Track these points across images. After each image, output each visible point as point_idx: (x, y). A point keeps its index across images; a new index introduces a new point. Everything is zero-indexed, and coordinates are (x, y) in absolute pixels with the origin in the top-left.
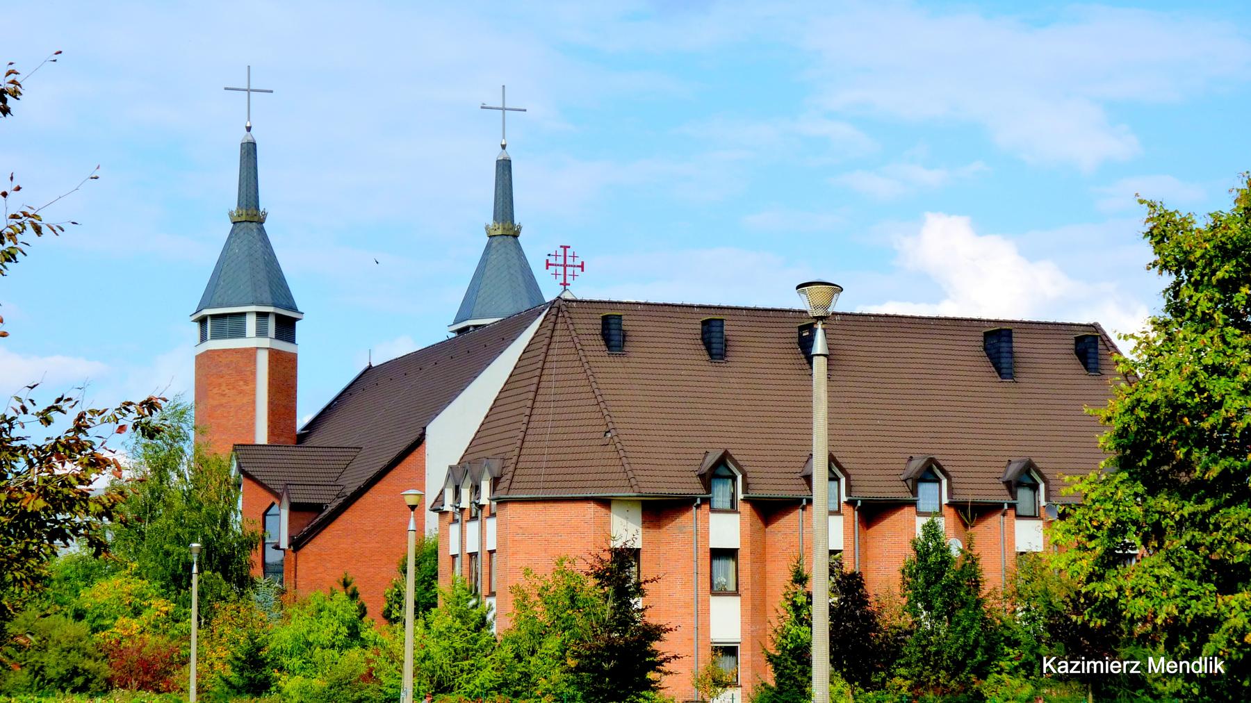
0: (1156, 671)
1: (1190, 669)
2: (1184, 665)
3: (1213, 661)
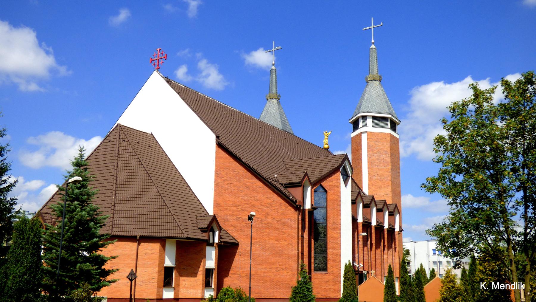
0: (496, 288)
1: (510, 288)
2: (508, 286)
3: (520, 284)
